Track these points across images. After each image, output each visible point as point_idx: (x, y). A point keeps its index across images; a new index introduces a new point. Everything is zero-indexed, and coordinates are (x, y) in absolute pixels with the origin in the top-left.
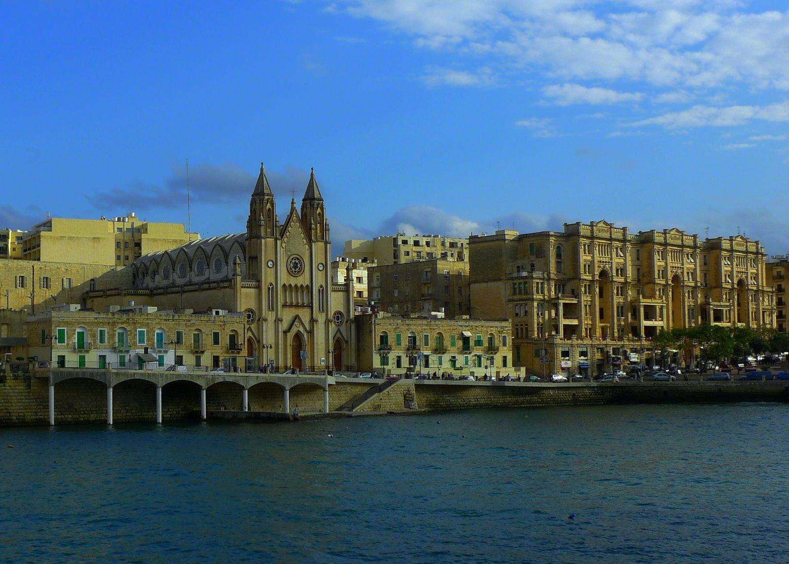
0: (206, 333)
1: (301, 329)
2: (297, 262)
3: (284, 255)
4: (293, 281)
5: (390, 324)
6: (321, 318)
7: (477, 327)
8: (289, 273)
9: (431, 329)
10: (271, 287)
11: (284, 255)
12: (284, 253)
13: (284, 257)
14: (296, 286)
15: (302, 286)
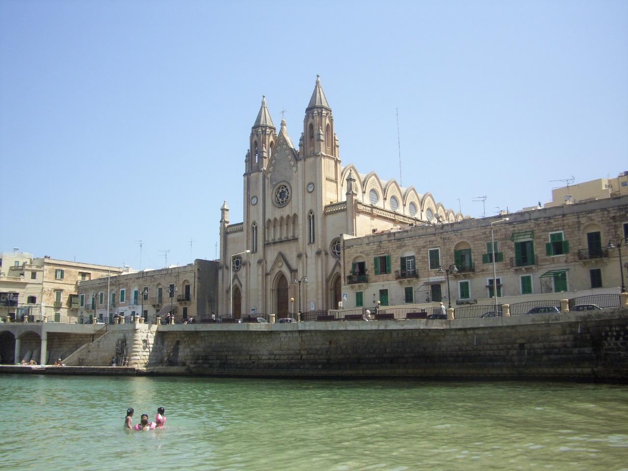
0: (165, 286)
1: (285, 270)
2: (284, 190)
3: (269, 186)
4: (279, 213)
5: (368, 244)
6: (311, 252)
7: (550, 218)
8: (274, 204)
9: (444, 239)
10: (254, 227)
11: (269, 186)
12: (269, 184)
13: (269, 188)
14: (282, 218)
15: (288, 217)
